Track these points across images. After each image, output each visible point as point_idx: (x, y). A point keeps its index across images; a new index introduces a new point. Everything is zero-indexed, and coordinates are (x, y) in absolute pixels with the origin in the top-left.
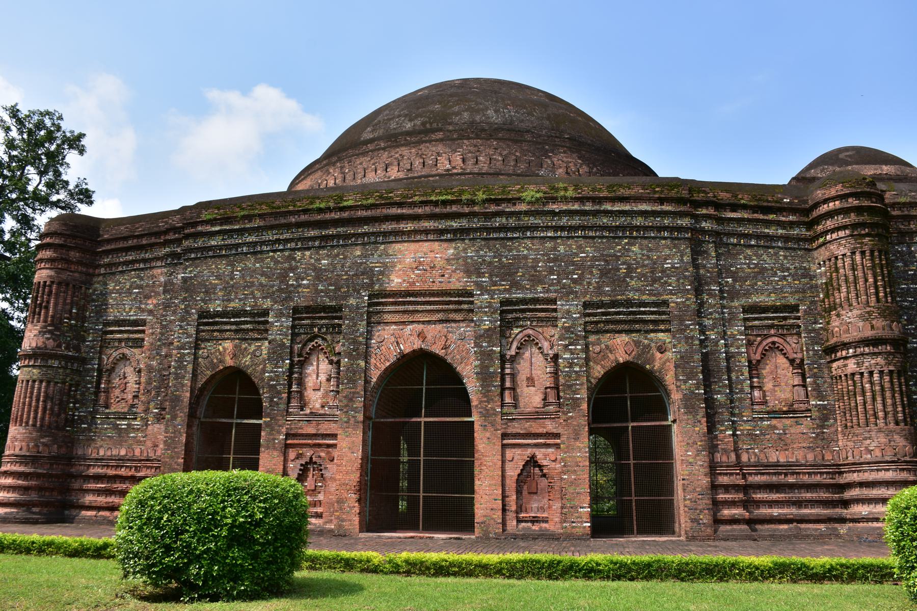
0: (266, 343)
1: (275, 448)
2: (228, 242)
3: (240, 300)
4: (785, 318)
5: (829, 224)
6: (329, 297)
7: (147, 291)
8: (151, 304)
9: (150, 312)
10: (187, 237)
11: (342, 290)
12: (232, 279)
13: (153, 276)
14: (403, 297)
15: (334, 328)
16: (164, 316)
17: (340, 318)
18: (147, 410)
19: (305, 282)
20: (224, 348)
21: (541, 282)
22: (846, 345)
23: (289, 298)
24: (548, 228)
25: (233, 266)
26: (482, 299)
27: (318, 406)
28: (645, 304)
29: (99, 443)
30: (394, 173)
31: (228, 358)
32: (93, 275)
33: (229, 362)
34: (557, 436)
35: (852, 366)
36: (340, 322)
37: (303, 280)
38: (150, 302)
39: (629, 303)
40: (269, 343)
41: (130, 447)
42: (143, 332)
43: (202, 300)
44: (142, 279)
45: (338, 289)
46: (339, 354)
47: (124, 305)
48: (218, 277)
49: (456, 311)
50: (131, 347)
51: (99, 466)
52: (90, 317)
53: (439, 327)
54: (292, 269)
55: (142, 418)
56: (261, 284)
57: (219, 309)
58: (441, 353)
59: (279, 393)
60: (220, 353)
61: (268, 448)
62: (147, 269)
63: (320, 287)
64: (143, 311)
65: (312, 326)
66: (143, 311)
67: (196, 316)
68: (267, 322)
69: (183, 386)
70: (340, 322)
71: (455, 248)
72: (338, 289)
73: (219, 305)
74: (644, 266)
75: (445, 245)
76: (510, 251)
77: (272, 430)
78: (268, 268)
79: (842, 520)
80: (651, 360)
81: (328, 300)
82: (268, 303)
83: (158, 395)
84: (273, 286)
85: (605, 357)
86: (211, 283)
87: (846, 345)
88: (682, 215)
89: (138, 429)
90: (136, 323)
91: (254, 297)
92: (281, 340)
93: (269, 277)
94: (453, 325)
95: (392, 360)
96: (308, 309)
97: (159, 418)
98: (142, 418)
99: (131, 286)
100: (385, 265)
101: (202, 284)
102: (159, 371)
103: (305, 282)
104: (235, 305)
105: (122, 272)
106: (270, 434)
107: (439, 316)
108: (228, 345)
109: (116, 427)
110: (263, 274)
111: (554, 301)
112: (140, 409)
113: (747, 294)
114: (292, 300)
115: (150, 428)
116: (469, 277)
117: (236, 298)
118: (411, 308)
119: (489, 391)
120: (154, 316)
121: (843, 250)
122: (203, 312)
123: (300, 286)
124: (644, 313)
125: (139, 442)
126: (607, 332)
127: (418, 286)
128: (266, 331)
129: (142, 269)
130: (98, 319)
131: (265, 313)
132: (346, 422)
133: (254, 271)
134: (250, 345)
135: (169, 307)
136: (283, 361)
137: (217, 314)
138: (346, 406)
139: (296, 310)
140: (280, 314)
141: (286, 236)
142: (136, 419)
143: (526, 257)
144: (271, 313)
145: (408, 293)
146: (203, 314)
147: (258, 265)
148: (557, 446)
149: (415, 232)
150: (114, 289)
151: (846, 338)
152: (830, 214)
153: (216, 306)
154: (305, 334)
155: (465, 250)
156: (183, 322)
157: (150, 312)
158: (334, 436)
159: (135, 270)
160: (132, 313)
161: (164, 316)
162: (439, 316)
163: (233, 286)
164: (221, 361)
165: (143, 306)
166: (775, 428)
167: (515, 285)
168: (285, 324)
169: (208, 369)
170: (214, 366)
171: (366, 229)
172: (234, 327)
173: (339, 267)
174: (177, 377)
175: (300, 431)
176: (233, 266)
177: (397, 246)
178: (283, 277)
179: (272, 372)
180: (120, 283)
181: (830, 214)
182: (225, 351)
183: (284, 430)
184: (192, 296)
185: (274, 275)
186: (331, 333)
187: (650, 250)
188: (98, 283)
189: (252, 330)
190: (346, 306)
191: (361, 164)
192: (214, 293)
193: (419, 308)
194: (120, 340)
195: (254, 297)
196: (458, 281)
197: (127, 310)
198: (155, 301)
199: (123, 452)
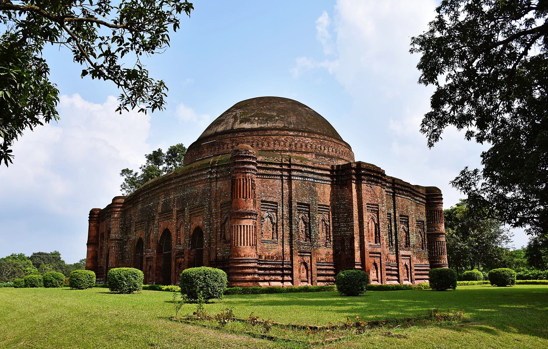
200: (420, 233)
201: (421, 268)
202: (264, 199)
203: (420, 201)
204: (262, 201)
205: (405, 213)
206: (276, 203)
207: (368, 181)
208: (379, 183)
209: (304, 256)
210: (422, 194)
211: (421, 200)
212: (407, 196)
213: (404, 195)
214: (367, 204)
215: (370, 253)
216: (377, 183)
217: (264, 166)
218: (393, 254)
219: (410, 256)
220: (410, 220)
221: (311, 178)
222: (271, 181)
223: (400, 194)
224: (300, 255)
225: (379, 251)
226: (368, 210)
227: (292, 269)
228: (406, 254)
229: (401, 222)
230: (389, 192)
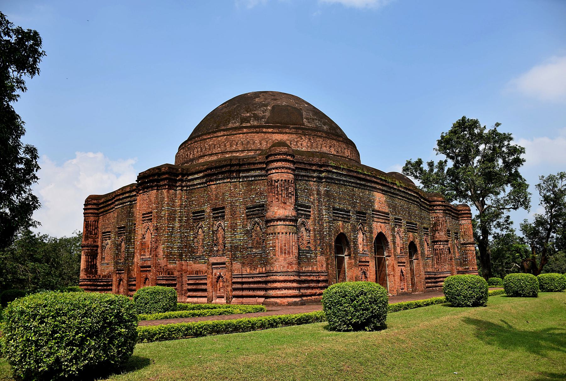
2: (339, 178)
5: (438, 207)
18: (316, 250)
21: (399, 213)
22: (441, 241)
26: (391, 216)
28: (413, 224)
29: (302, 265)
30: (333, 152)
35: (442, 247)
68: (350, 215)
72: (365, 206)
79: (436, 287)
87: (441, 241)
88: (418, 198)
97: (322, 253)
105: (300, 180)
107: (383, 221)
111: (401, 220)
112: (313, 248)
121: (441, 216)
141: (352, 180)
148: (404, 266)
151: (440, 239)
152: (439, 205)
153: (337, 206)
158: (368, 262)
162: (383, 221)
171: (369, 184)
181: (439, 205)
194: (302, 214)
196: (387, 210)
200: (258, 224)
201: (251, 280)
202: (104, 231)
203: (255, 176)
204: (104, 233)
205: (220, 204)
206: (110, 232)
207: (143, 189)
208: (154, 187)
209: (119, 273)
210: (260, 163)
211: (258, 173)
212: (223, 179)
213: (220, 179)
214: (143, 214)
215: (142, 267)
216: (152, 188)
217: (105, 204)
218: (205, 263)
219: (224, 263)
220: (227, 211)
221: (127, 202)
222: (108, 215)
223: (212, 181)
224: (119, 273)
225: (149, 264)
226: (144, 221)
227: (111, 285)
228: (219, 261)
229: (214, 217)
230: (202, 183)
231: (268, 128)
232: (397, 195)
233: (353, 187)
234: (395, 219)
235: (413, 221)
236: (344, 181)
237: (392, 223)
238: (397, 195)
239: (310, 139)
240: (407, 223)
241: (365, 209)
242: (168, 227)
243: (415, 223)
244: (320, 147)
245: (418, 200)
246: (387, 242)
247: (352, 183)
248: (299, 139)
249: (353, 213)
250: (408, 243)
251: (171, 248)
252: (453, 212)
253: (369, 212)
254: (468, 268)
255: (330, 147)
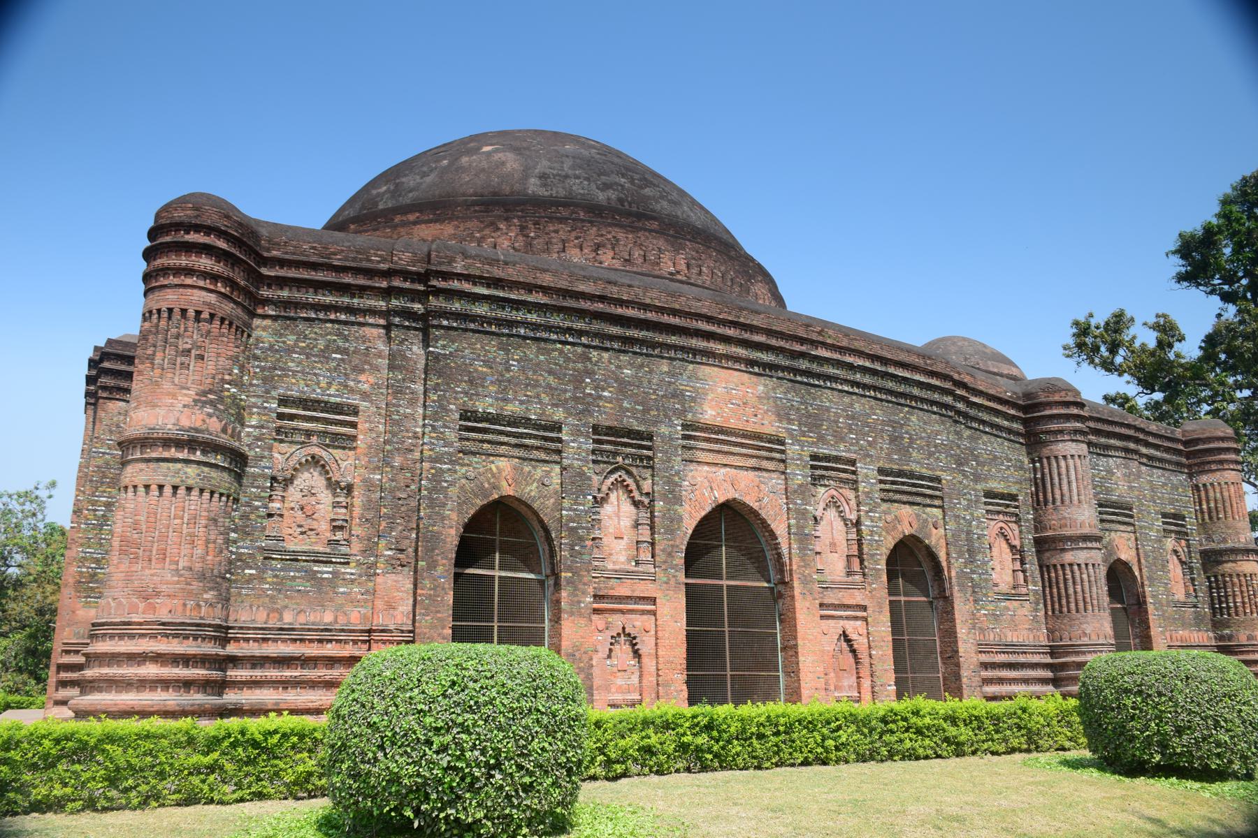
0: (557, 469)
1: (581, 615)
3: (522, 402)
4: (1008, 506)
6: (637, 419)
7: (356, 361)
8: (366, 381)
9: (365, 396)
10: (438, 292)
11: (652, 413)
12: (508, 370)
13: (364, 339)
14: (715, 433)
15: (642, 460)
16: (394, 405)
17: (649, 448)
18: (370, 549)
19: (606, 394)
20: (497, 467)
21: (842, 439)
23: (587, 411)
24: (846, 381)
25: (507, 351)
26: (793, 450)
27: (623, 559)
31: (504, 484)
32: (253, 315)
33: (507, 490)
34: (864, 608)
36: (650, 453)
37: (603, 390)
38: (362, 378)
39: (911, 475)
40: (564, 469)
41: (339, 609)
42: (354, 425)
43: (466, 393)
44: (346, 339)
45: (646, 411)
46: (648, 494)
47: (315, 374)
48: (487, 363)
49: (768, 459)
50: (328, 446)
51: (284, 641)
52: (251, 385)
53: (751, 474)
54: (590, 373)
55: (359, 564)
56: (549, 386)
57: (491, 410)
58: (755, 506)
59: (581, 539)
60: (494, 476)
61: (571, 614)
62: (353, 324)
63: (625, 404)
64: (352, 391)
65: (615, 454)
66: (352, 391)
67: (457, 416)
68: (560, 440)
69: (443, 518)
70: (650, 453)
71: (766, 386)
72: (646, 411)
73: (491, 405)
74: (921, 438)
75: (754, 378)
76: (814, 399)
77: (576, 589)
78: (556, 364)
80: (929, 536)
81: (635, 423)
82: (559, 415)
83: (392, 529)
84: (566, 391)
85: (894, 528)
86: (476, 370)
89: (353, 581)
90: (338, 409)
91: (540, 402)
92: (580, 468)
93: (559, 379)
94: (765, 474)
95: (708, 509)
96: (611, 431)
98: (359, 564)
99: (327, 347)
100: (696, 390)
101: (464, 369)
102: (392, 491)
103: (606, 394)
104: (513, 408)
106: (573, 594)
108: (502, 463)
109: (312, 576)
110: (550, 372)
111: (853, 463)
113: (986, 480)
114: (592, 416)
115: (379, 580)
116: (780, 421)
117: (515, 399)
118: (726, 448)
119: (806, 555)
120: (371, 401)
122: (466, 411)
123: (600, 397)
124: (922, 486)
125: (355, 602)
126: (895, 501)
127: (733, 423)
128: (559, 452)
129: (345, 323)
130: (267, 392)
131: (557, 427)
132: (666, 583)
133: (538, 364)
134: (534, 467)
135: (401, 392)
136: (585, 497)
137: (487, 418)
138: (665, 562)
139: (596, 429)
140: (576, 433)
142: (348, 563)
143: (828, 409)
144: (565, 429)
145: (721, 430)
146: (467, 415)
147: (542, 358)
149: (728, 357)
150: (296, 345)
153: (486, 405)
154: (605, 462)
155: (774, 389)
156: (436, 421)
157: (365, 396)
159: (332, 321)
160: (332, 391)
161: (394, 405)
163: (509, 381)
164: (495, 487)
165: (351, 383)
166: (1007, 609)
167: (821, 439)
168: (584, 447)
169: (476, 496)
170: (484, 492)
172: (513, 441)
173: (645, 384)
174: (432, 503)
175: (611, 593)
176: (507, 351)
177: (707, 369)
178: (578, 381)
179: (570, 509)
180: (305, 337)
182: (504, 474)
183: (591, 590)
184: (448, 384)
185: (565, 375)
186: (637, 466)
187: (925, 423)
188: (264, 329)
189: (537, 448)
190: (659, 435)
191: (556, 232)
192: (483, 386)
193: (737, 450)
194: (308, 434)
195: (540, 402)
196: (770, 425)
197: (323, 384)
198: (372, 380)
199: (328, 618)
231: (406, 213)
232: (834, 379)
233: (585, 346)
234: (814, 457)
235: (915, 467)
236: (535, 327)
237: (800, 476)
238: (834, 379)
239: (523, 228)
240: (881, 471)
241: (642, 421)
242: (94, 503)
243: (925, 472)
244: (557, 247)
245: (948, 400)
246: (773, 536)
247: (581, 333)
248: (487, 232)
249: (576, 433)
250: (890, 543)
251: (97, 561)
252: (1147, 444)
253: (664, 429)
254: (1230, 638)
255: (597, 247)
